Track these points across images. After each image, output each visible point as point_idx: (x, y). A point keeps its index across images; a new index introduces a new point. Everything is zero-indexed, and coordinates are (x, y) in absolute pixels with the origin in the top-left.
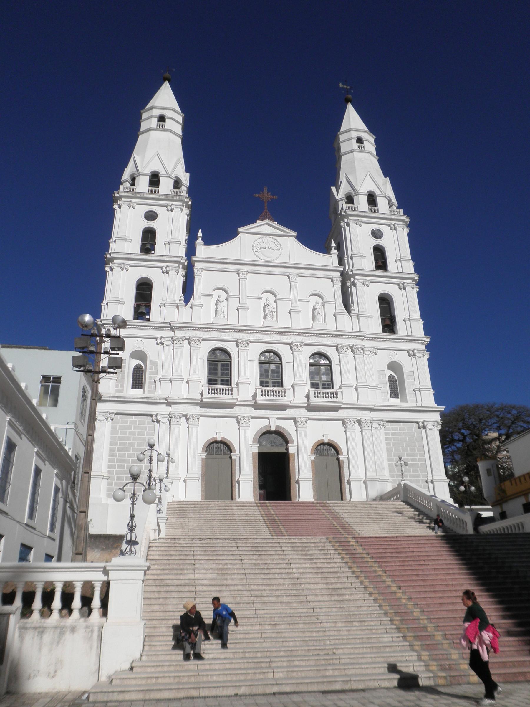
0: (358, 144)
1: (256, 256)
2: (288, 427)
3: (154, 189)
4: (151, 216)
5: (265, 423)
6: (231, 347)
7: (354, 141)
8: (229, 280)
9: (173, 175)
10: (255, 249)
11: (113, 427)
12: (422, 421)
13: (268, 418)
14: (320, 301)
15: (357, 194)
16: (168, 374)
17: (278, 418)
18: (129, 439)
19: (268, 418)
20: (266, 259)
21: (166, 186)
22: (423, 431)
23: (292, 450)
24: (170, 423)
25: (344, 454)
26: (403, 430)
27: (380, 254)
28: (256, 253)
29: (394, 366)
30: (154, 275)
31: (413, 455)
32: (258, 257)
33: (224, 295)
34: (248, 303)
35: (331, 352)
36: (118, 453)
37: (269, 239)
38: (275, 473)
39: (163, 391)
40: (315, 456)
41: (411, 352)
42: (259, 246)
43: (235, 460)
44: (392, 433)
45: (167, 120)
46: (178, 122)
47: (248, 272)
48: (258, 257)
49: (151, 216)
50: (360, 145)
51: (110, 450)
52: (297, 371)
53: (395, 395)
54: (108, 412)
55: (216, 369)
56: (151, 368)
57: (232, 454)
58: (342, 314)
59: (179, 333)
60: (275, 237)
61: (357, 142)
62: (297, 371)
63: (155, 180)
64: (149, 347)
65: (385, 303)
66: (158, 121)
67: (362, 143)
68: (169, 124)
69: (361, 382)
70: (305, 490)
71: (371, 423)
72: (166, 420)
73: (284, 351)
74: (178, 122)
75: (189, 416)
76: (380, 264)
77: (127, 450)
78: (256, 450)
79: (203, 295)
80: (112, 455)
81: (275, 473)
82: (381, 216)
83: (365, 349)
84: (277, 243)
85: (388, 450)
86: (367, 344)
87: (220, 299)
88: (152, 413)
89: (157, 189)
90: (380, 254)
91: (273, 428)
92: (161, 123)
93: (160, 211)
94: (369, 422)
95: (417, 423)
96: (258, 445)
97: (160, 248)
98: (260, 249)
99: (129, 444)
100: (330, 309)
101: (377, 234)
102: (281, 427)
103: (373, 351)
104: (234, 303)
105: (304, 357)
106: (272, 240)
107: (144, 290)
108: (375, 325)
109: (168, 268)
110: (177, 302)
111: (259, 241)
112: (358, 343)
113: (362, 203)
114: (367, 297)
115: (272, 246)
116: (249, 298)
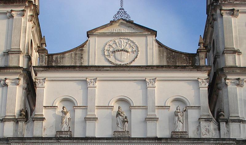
1: (108, 60)
10: (106, 53)
20: (119, 63)
42: (111, 49)
48: (110, 62)
58: (208, 120)
60: (131, 39)
98: (114, 52)
100: (193, 115)
106: (126, 41)
109: (7, 81)
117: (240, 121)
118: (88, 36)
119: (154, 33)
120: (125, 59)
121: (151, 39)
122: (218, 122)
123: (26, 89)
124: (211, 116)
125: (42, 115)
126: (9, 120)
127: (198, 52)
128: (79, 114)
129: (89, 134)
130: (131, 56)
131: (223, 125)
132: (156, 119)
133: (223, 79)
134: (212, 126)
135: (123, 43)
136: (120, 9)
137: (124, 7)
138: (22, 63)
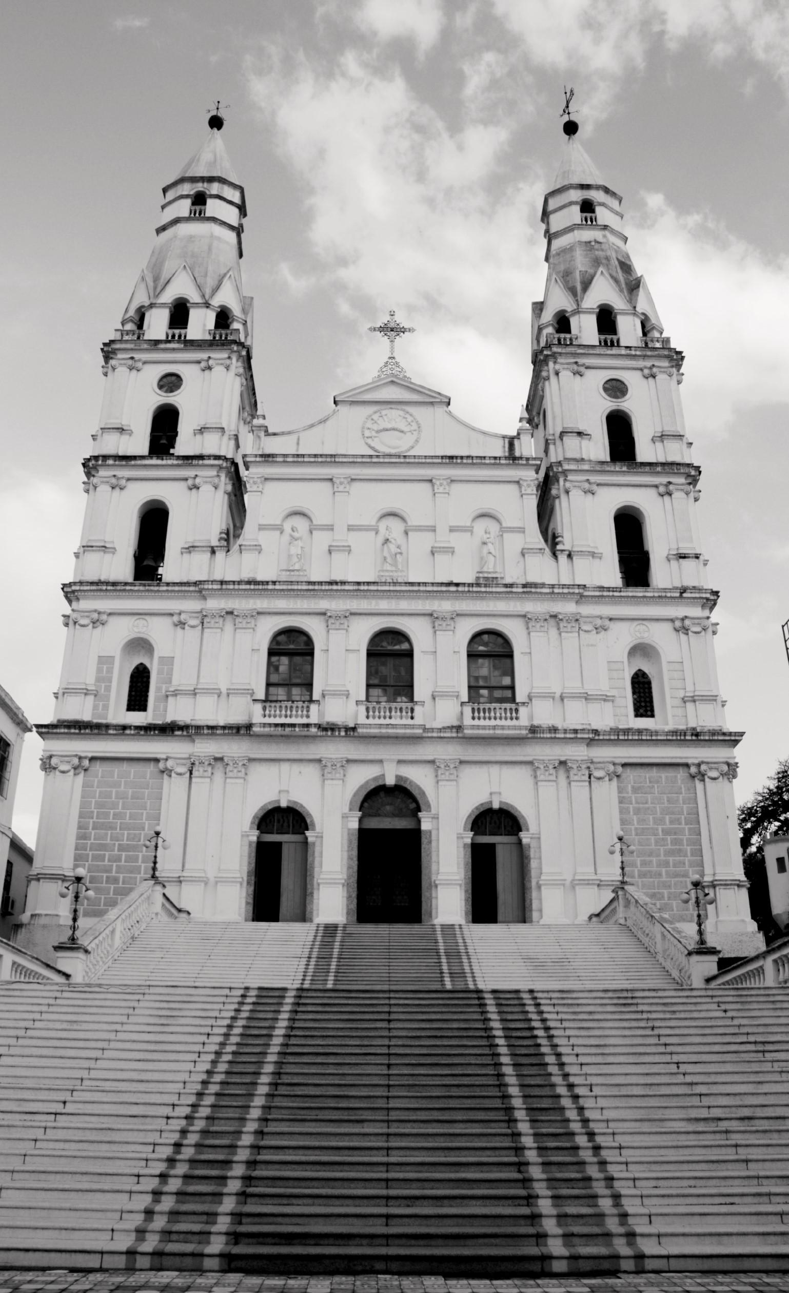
0: (585, 215)
2: (420, 778)
3: (177, 332)
4: (171, 382)
6: (314, 627)
7: (577, 209)
8: (312, 496)
9: (216, 302)
11: (85, 785)
12: (696, 761)
15: (577, 312)
17: (400, 762)
18: (114, 806)
21: (200, 324)
23: (425, 826)
24: (191, 773)
25: (531, 831)
26: (658, 782)
27: (620, 429)
28: (369, 441)
35: (513, 630)
36: (93, 832)
38: (389, 869)
39: (179, 711)
40: (471, 834)
41: (678, 624)
42: (375, 427)
43: (314, 844)
44: (633, 787)
45: (210, 202)
46: (231, 203)
49: (171, 382)
50: (589, 215)
51: (80, 828)
52: (440, 668)
53: (646, 711)
54: (76, 756)
56: (160, 672)
57: (308, 833)
59: (214, 604)
61: (582, 211)
62: (440, 668)
63: (180, 314)
64: (160, 633)
65: (629, 526)
66: (193, 204)
67: (593, 211)
68: (213, 207)
69: (574, 686)
70: (448, 901)
71: (589, 768)
72: (183, 769)
73: (419, 634)
74: (231, 203)
75: (226, 759)
77: (112, 828)
78: (354, 825)
79: (262, 528)
80: (82, 836)
81: (389, 869)
82: (623, 352)
83: (582, 620)
84: (410, 419)
86: (587, 610)
87: (296, 535)
88: (158, 756)
89: (183, 331)
90: (620, 429)
91: (390, 781)
92: (198, 208)
93: (187, 372)
94: (584, 766)
95: (687, 765)
96: (359, 814)
97: (185, 444)
99: (114, 815)
100: (514, 543)
101: (616, 388)
102: (406, 779)
104: (322, 540)
105: (361, 633)
106: (401, 413)
108: (608, 571)
110: (215, 542)
111: (375, 417)
112: (568, 608)
113: (586, 328)
115: (402, 425)
116: (351, 528)
117: (593, 555)
118: (335, 402)
121: (440, 411)
123: (229, 494)
124: (542, 544)
125: (257, 540)
127: (519, 434)
132: (451, 551)
135: (393, 417)
136: (390, 358)
137: (395, 355)
138: (227, 450)
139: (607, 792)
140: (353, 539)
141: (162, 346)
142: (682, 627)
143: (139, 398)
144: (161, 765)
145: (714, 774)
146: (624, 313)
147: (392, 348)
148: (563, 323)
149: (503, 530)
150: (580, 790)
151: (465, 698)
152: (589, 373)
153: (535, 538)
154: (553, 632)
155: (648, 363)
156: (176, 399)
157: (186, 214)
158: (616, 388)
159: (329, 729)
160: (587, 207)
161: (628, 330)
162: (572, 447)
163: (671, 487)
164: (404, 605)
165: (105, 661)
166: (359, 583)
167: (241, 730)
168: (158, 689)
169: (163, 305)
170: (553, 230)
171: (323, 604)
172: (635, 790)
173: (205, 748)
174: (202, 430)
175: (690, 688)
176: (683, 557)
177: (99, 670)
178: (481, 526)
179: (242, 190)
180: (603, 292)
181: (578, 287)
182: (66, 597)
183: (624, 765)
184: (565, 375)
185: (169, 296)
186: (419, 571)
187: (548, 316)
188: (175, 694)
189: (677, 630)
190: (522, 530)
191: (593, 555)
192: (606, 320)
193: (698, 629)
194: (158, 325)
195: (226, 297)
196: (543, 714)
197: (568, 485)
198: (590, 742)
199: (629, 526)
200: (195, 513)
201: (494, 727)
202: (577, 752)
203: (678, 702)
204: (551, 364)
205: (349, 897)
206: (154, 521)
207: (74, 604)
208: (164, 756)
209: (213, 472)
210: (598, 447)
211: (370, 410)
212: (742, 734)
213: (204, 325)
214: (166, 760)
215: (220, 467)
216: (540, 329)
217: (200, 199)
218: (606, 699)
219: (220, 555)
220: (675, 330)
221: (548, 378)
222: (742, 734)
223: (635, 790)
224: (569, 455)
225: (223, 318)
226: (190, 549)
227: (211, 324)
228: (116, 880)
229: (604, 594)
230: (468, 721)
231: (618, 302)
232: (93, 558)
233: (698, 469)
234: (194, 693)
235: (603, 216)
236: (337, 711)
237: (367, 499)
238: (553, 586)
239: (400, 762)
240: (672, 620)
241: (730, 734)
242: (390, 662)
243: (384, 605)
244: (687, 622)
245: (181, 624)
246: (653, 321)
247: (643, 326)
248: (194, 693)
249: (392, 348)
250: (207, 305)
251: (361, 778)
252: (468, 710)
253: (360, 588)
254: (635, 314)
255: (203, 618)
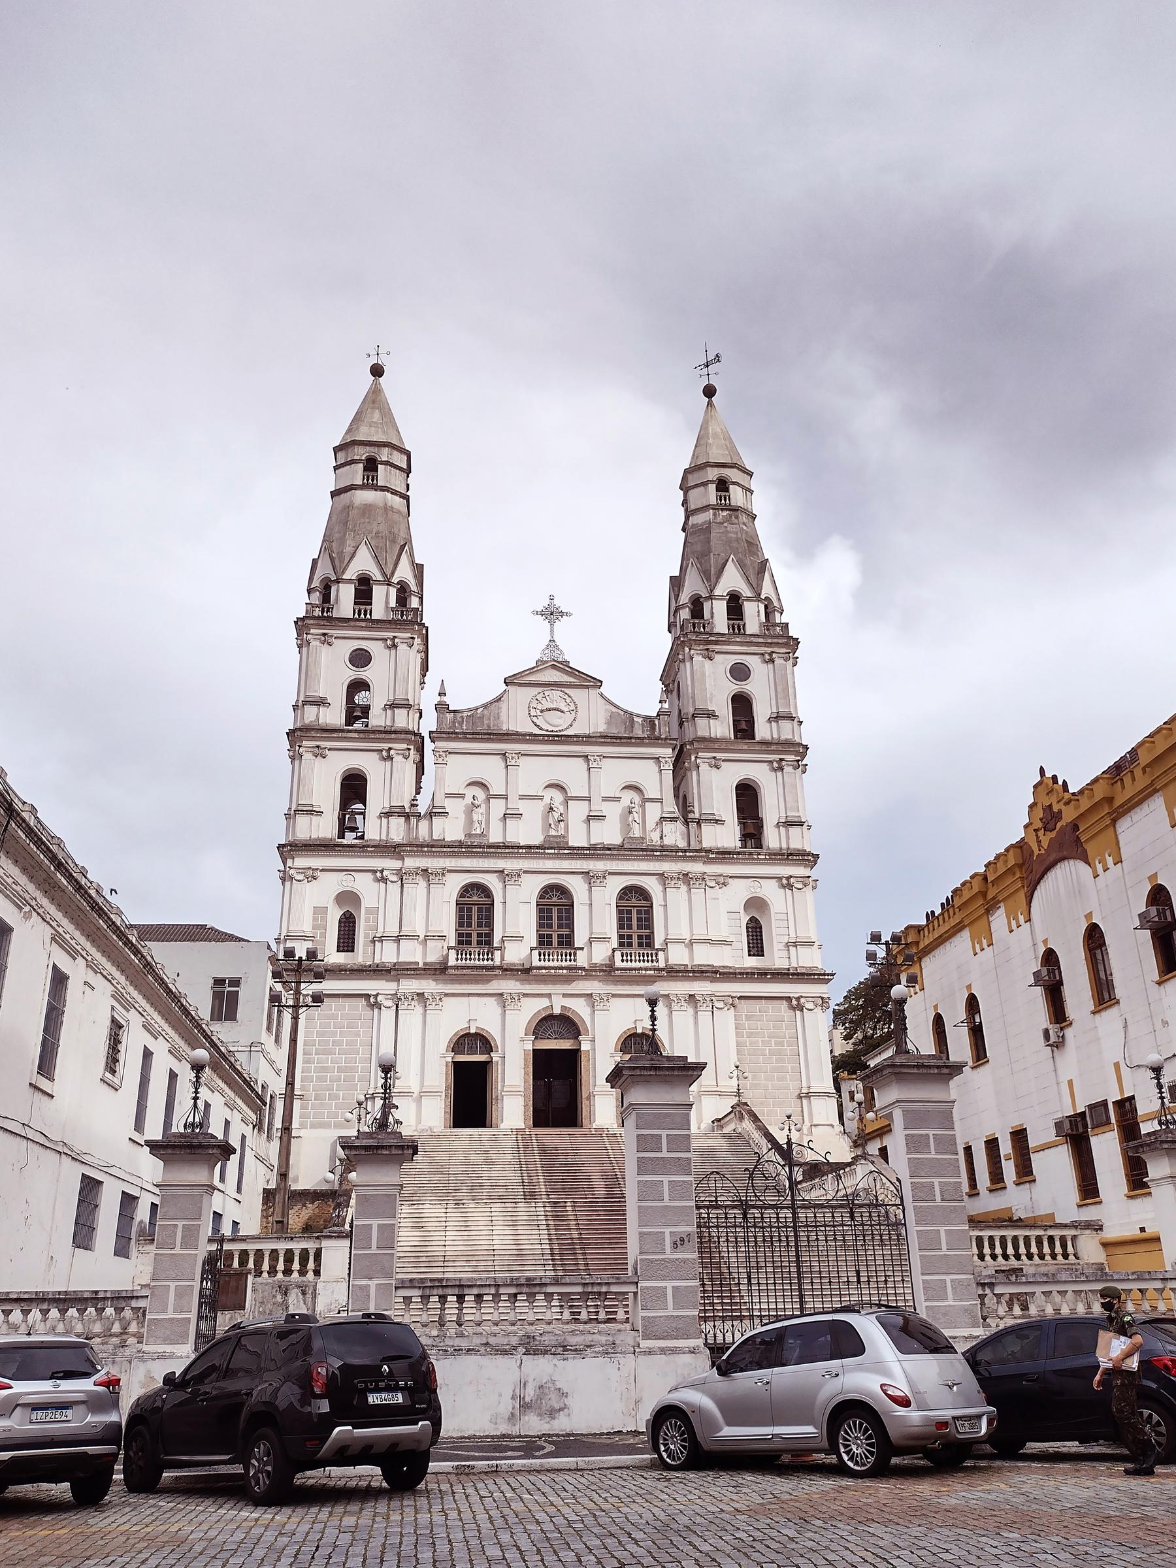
2: (580, 1008)
4: (360, 659)
5: (545, 1002)
7: (712, 488)
9: (395, 580)
10: (533, 713)
12: (796, 996)
13: (549, 996)
14: (637, 799)
15: (710, 598)
16: (393, 930)
17: (564, 995)
18: (334, 1034)
19: (549, 996)
21: (382, 601)
22: (798, 1012)
27: (742, 705)
28: (535, 719)
29: (756, 904)
30: (368, 763)
31: (780, 1052)
32: (538, 726)
33: (480, 794)
34: (522, 806)
35: (652, 886)
37: (556, 694)
41: (785, 881)
42: (540, 707)
47: (521, 754)
48: (538, 726)
49: (360, 659)
52: (596, 920)
55: (470, 917)
56: (367, 921)
59: (411, 863)
60: (566, 690)
62: (596, 920)
64: (364, 885)
65: (747, 795)
67: (727, 490)
69: (700, 933)
73: (576, 885)
76: (744, 726)
77: (331, 1053)
81: (557, 1085)
84: (568, 700)
85: (738, 1044)
89: (368, 607)
90: (742, 705)
91: (557, 1011)
92: (371, 474)
93: (376, 649)
95: (789, 999)
100: (654, 812)
101: (740, 672)
103: (722, 882)
104: (498, 807)
107: (354, 787)
108: (728, 835)
109: (392, 752)
110: (407, 810)
113: (718, 614)
114: (716, 787)
116: (523, 797)
117: (717, 821)
119: (598, 683)
120: (557, 723)
121: (593, 692)
122: (686, 822)
126: (400, 815)
128: (498, 807)
129: (511, 838)
130: (568, 718)
131: (693, 826)
133: (693, 758)
134: (679, 826)
135: (555, 698)
139: (726, 1018)
140: (522, 806)
141: (352, 623)
142: (787, 884)
143: (333, 673)
144: (372, 1000)
145: (810, 1006)
146: (749, 599)
147: (552, 631)
148: (697, 606)
149: (645, 800)
150: (705, 1017)
151: (615, 943)
152: (718, 657)
153: (671, 806)
154: (684, 888)
155: (769, 650)
156: (365, 674)
157: (359, 481)
158: (740, 672)
159: (508, 971)
160: (723, 485)
161: (753, 615)
162: (704, 728)
163: (784, 763)
164: (566, 865)
165: (320, 911)
166: (530, 847)
167: (439, 970)
168: (366, 936)
169: (350, 581)
170: (692, 507)
171: (501, 864)
172: (748, 1018)
173: (410, 986)
174: (393, 706)
175: (793, 934)
176: (789, 824)
177: (315, 919)
178: (628, 796)
179: (408, 454)
180: (732, 580)
181: (711, 577)
182: (281, 855)
183: (740, 998)
184: (698, 659)
185: (351, 573)
186: (577, 839)
187: (684, 598)
188: (381, 939)
189: (784, 887)
190: (660, 801)
191: (717, 821)
192: (735, 605)
193: (800, 886)
194: (345, 598)
195: (404, 572)
196: (678, 956)
197: (699, 761)
198: (714, 980)
199: (747, 795)
200: (388, 782)
201: (640, 969)
202: (701, 988)
203: (781, 946)
204: (687, 649)
205: (526, 1106)
206: (354, 787)
207: (289, 863)
208: (375, 993)
209: (405, 746)
210: (723, 728)
211: (536, 690)
212: (833, 974)
213: (387, 602)
214: (377, 995)
215: (409, 742)
216: (677, 610)
217: (371, 465)
218: (724, 943)
219: (413, 820)
220: (794, 617)
221: (684, 661)
222: (833, 974)
223: (748, 1018)
224: (700, 733)
225: (403, 592)
226: (388, 814)
227: (393, 603)
228: (337, 1097)
229: (724, 855)
230: (618, 963)
231: (746, 592)
232: (301, 820)
233: (806, 747)
234: (397, 939)
235: (736, 496)
236: (515, 954)
237: (533, 772)
238: (685, 851)
239: (564, 995)
240: (780, 879)
241: (824, 974)
242: (556, 911)
243: (549, 864)
244: (792, 880)
245: (384, 880)
246: (776, 604)
247: (766, 607)
248: (397, 939)
249: (552, 631)
250: (388, 582)
251: (532, 1009)
252: (618, 954)
253: (530, 851)
254: (759, 600)
255: (401, 874)
